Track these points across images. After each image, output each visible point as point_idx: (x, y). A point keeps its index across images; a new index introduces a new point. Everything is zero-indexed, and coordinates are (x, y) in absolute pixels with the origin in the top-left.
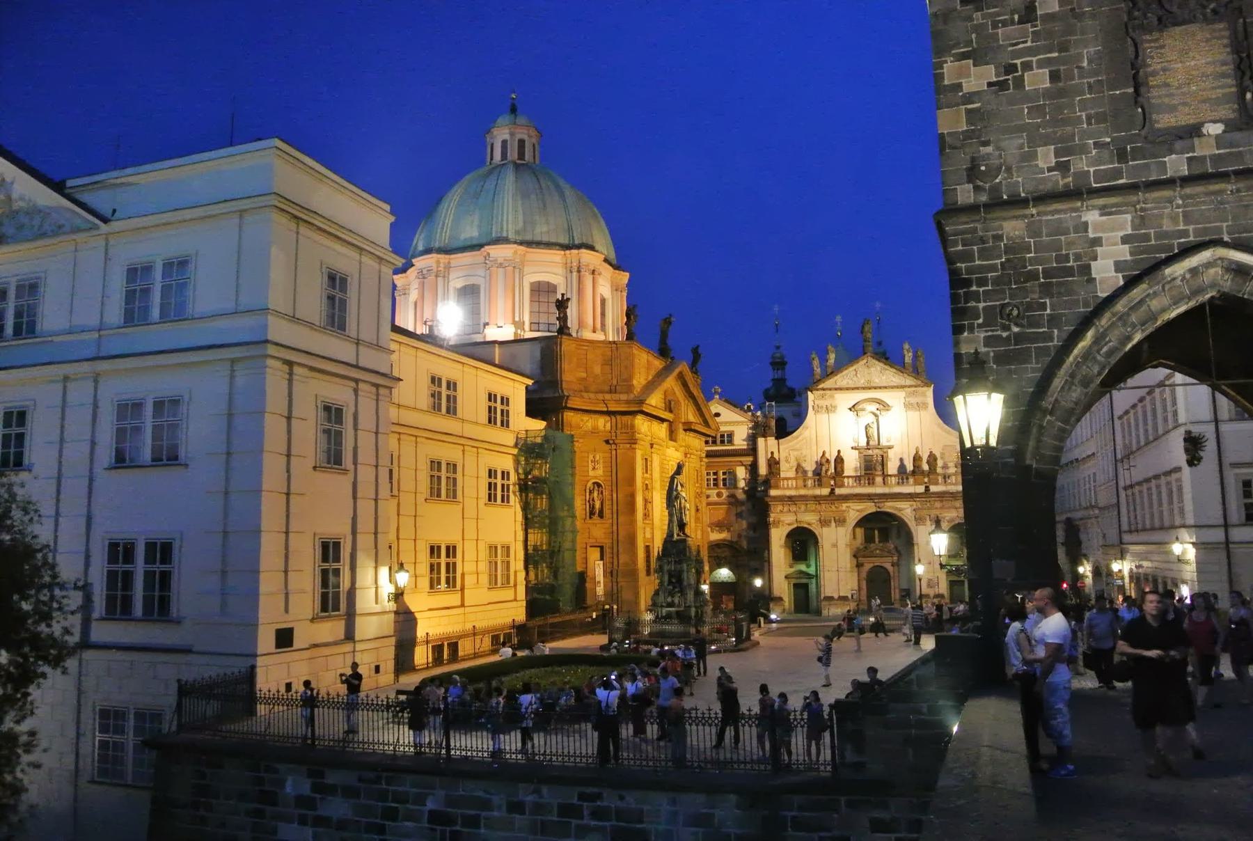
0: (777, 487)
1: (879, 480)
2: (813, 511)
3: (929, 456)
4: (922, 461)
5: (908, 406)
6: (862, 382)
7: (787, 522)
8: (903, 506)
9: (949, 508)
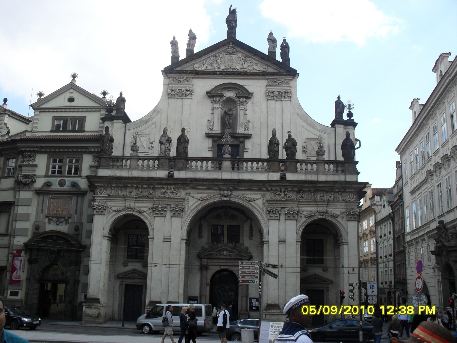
0: (107, 167)
1: (227, 164)
2: (146, 197)
3: (287, 141)
4: (278, 145)
5: (270, 95)
6: (223, 68)
7: (114, 208)
8: (253, 197)
9: (307, 201)
